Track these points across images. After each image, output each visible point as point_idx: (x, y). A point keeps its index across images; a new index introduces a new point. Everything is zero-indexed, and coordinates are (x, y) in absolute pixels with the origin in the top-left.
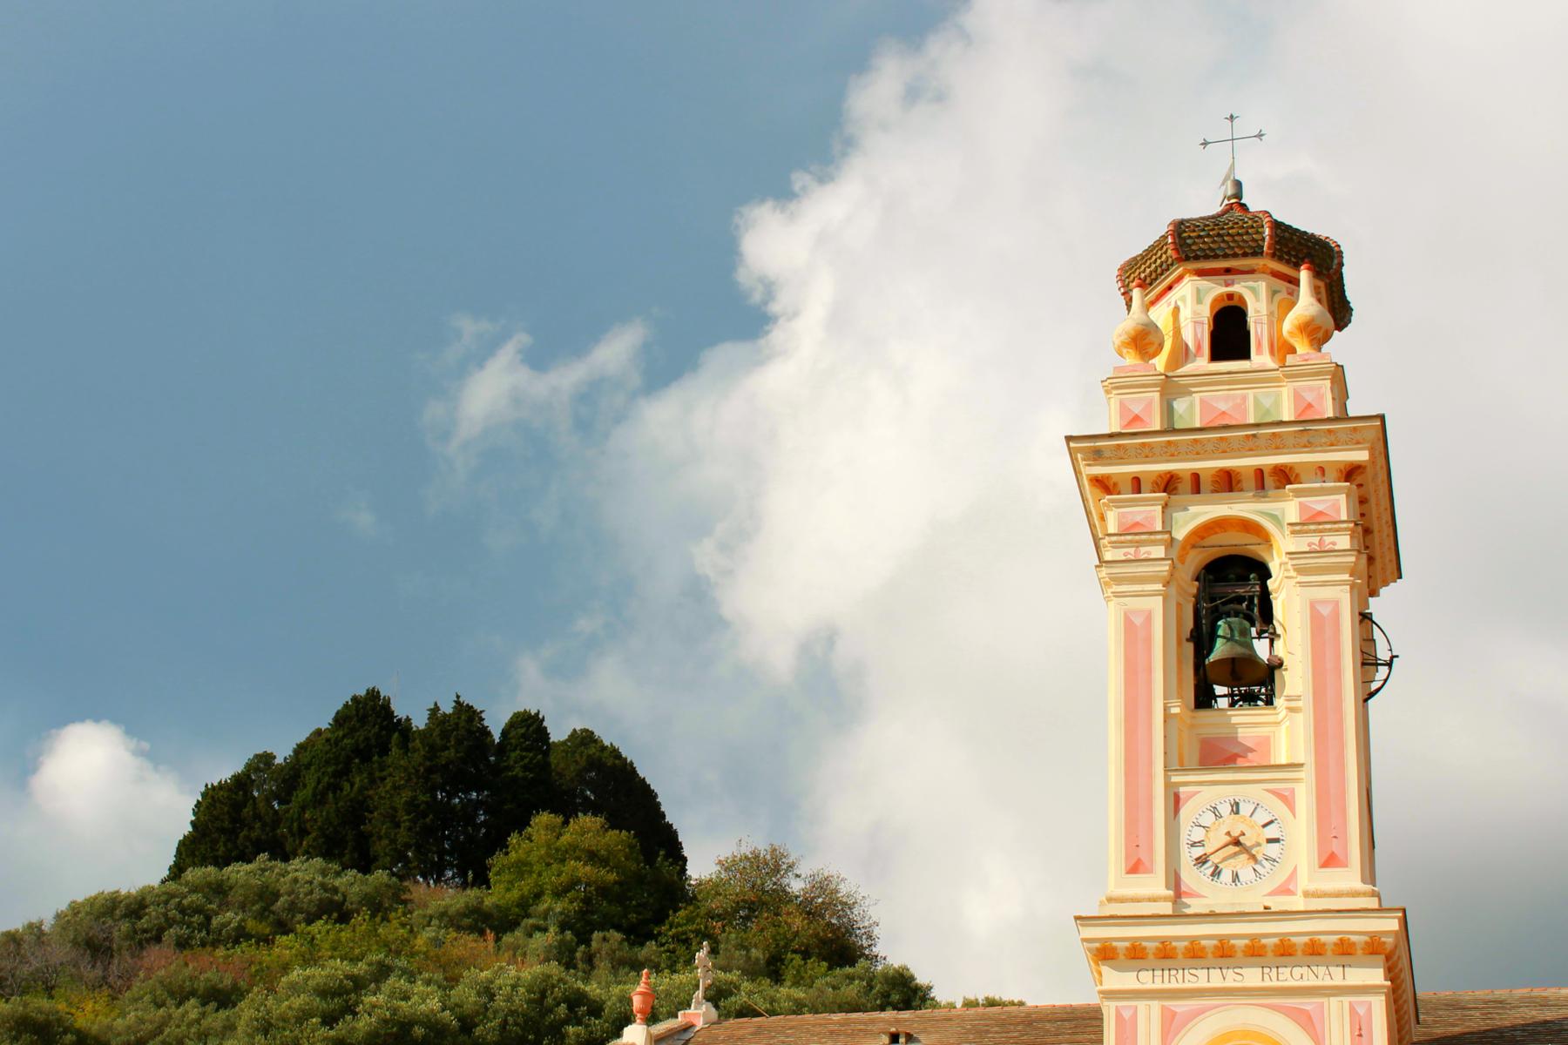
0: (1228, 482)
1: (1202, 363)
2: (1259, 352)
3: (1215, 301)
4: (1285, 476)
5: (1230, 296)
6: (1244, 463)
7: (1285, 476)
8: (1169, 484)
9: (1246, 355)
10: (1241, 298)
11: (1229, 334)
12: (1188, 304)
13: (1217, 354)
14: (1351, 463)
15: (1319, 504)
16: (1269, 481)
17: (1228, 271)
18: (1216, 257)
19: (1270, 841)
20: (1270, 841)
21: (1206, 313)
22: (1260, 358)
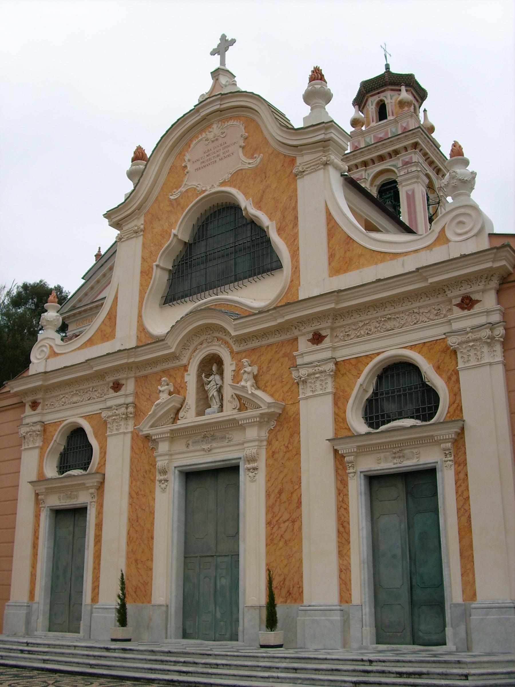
0: (381, 158)
3: (378, 103)
4: (396, 152)
5: (381, 101)
7: (396, 152)
8: (365, 164)
9: (386, 118)
14: (413, 144)
15: (407, 158)
16: (393, 155)
17: (378, 93)
21: (374, 106)
22: (390, 118)
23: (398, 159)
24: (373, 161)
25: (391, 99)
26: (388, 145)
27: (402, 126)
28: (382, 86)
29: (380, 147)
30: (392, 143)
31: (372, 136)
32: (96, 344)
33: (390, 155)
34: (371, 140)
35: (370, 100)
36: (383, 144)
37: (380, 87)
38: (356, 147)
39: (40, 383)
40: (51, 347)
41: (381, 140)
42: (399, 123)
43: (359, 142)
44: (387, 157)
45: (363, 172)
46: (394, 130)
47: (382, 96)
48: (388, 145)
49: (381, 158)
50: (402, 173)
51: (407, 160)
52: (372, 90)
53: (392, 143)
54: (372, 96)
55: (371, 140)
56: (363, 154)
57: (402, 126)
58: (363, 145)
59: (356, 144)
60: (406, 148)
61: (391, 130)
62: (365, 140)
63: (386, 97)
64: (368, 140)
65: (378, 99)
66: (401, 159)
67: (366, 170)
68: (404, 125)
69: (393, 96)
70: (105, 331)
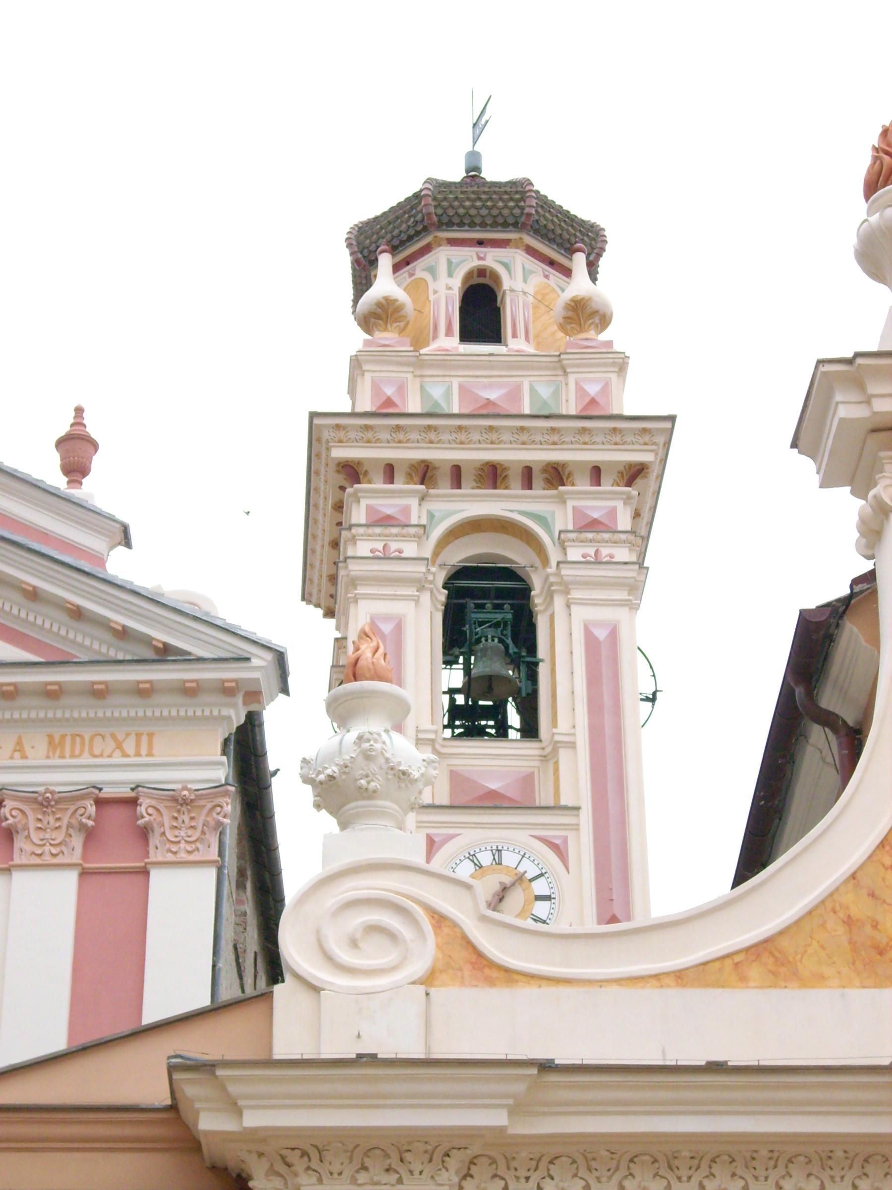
0: (493, 476)
1: (452, 343)
2: (515, 335)
3: (469, 275)
5: (482, 272)
6: (510, 455)
7: (556, 475)
8: (424, 473)
10: (496, 278)
11: (481, 311)
12: (445, 274)
13: (467, 336)
14: (630, 465)
15: (596, 508)
16: (537, 481)
17: (480, 243)
18: (472, 225)
19: (539, 898)
20: (539, 898)
21: (456, 285)
22: (515, 344)
23: (562, 500)
24: (457, 475)
25: (525, 281)
26: (538, 438)
27: (580, 390)
28: (505, 225)
29: (506, 437)
30: (555, 437)
31: (456, 383)
32: (819, 980)
33: (528, 476)
34: (448, 394)
35: (442, 255)
36: (522, 429)
37: (495, 224)
38: (389, 402)
39: (497, 1118)
40: (439, 919)
41: (489, 411)
42: (572, 379)
43: (401, 389)
44: (515, 480)
45: (414, 502)
46: (545, 392)
47: (492, 258)
48: (538, 438)
49: (493, 476)
50: (574, 554)
51: (596, 515)
52: (461, 224)
53: (555, 438)
54: (453, 242)
55: (448, 394)
56: (432, 436)
57: (580, 390)
58: (414, 405)
59: (389, 391)
60: (596, 473)
61: (532, 390)
62: (422, 388)
63: (506, 266)
64: (437, 392)
65: (476, 263)
66: (570, 504)
67: (423, 499)
68: (593, 389)
69: (531, 272)
70: (875, 926)
